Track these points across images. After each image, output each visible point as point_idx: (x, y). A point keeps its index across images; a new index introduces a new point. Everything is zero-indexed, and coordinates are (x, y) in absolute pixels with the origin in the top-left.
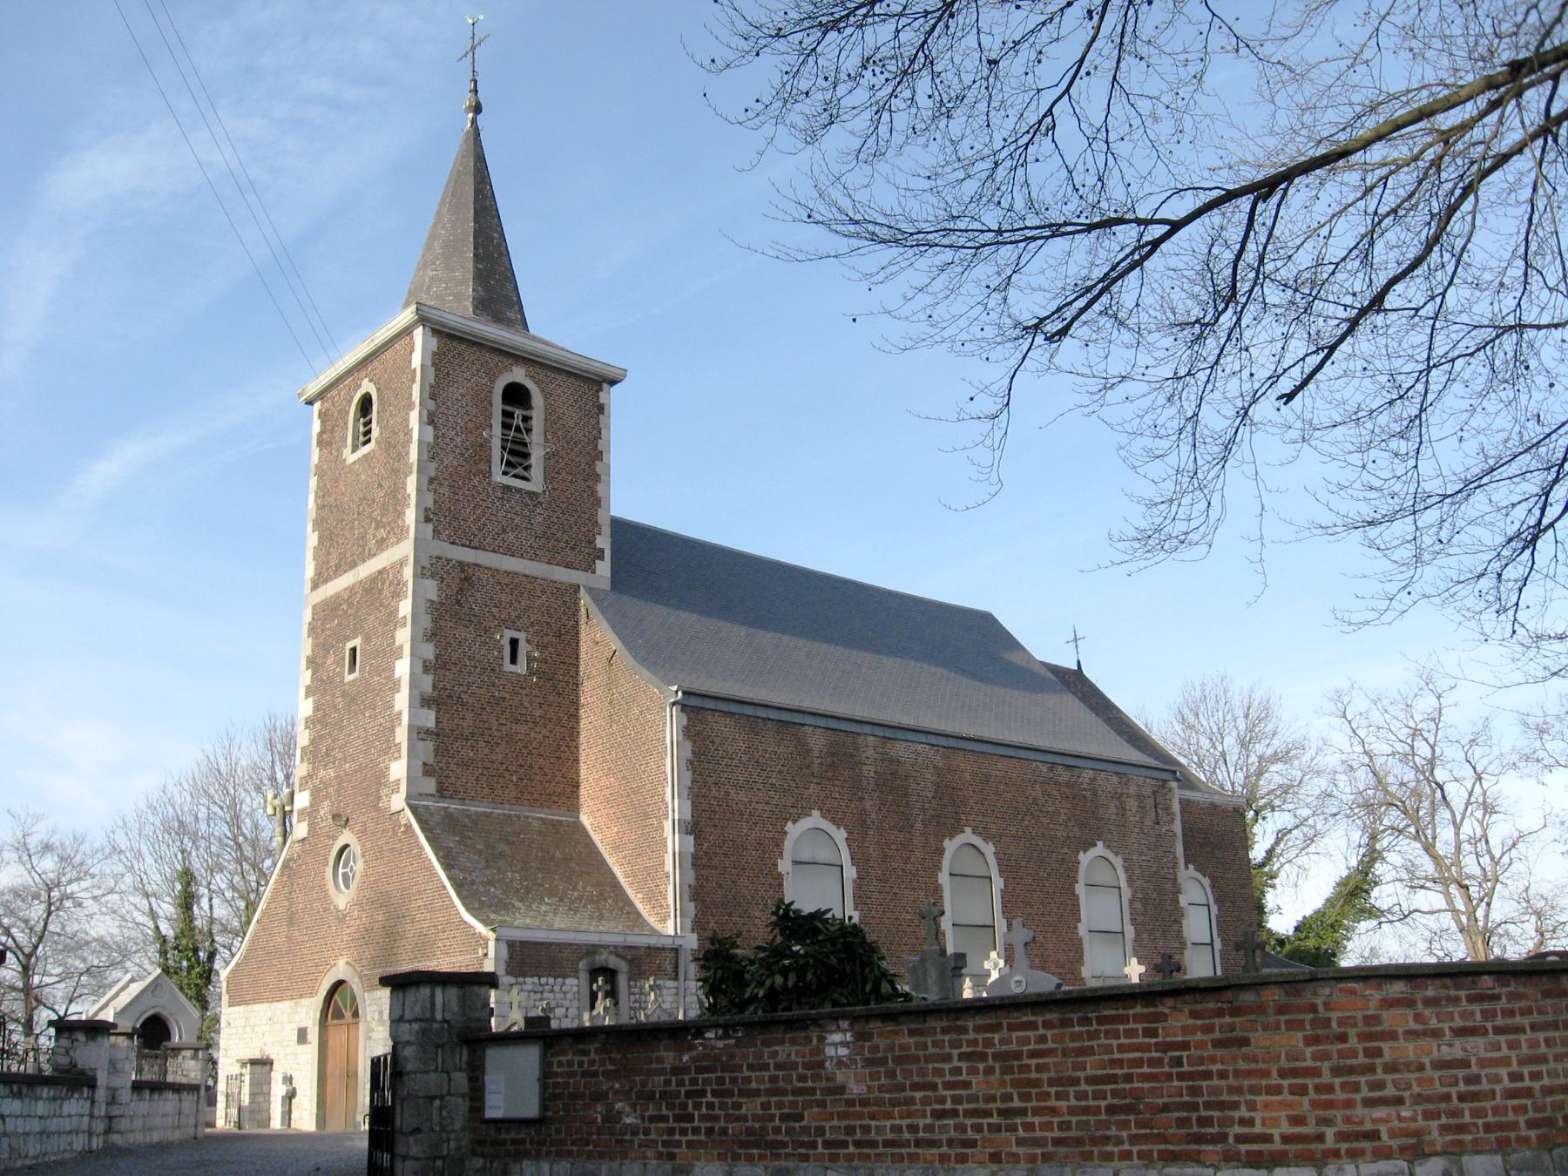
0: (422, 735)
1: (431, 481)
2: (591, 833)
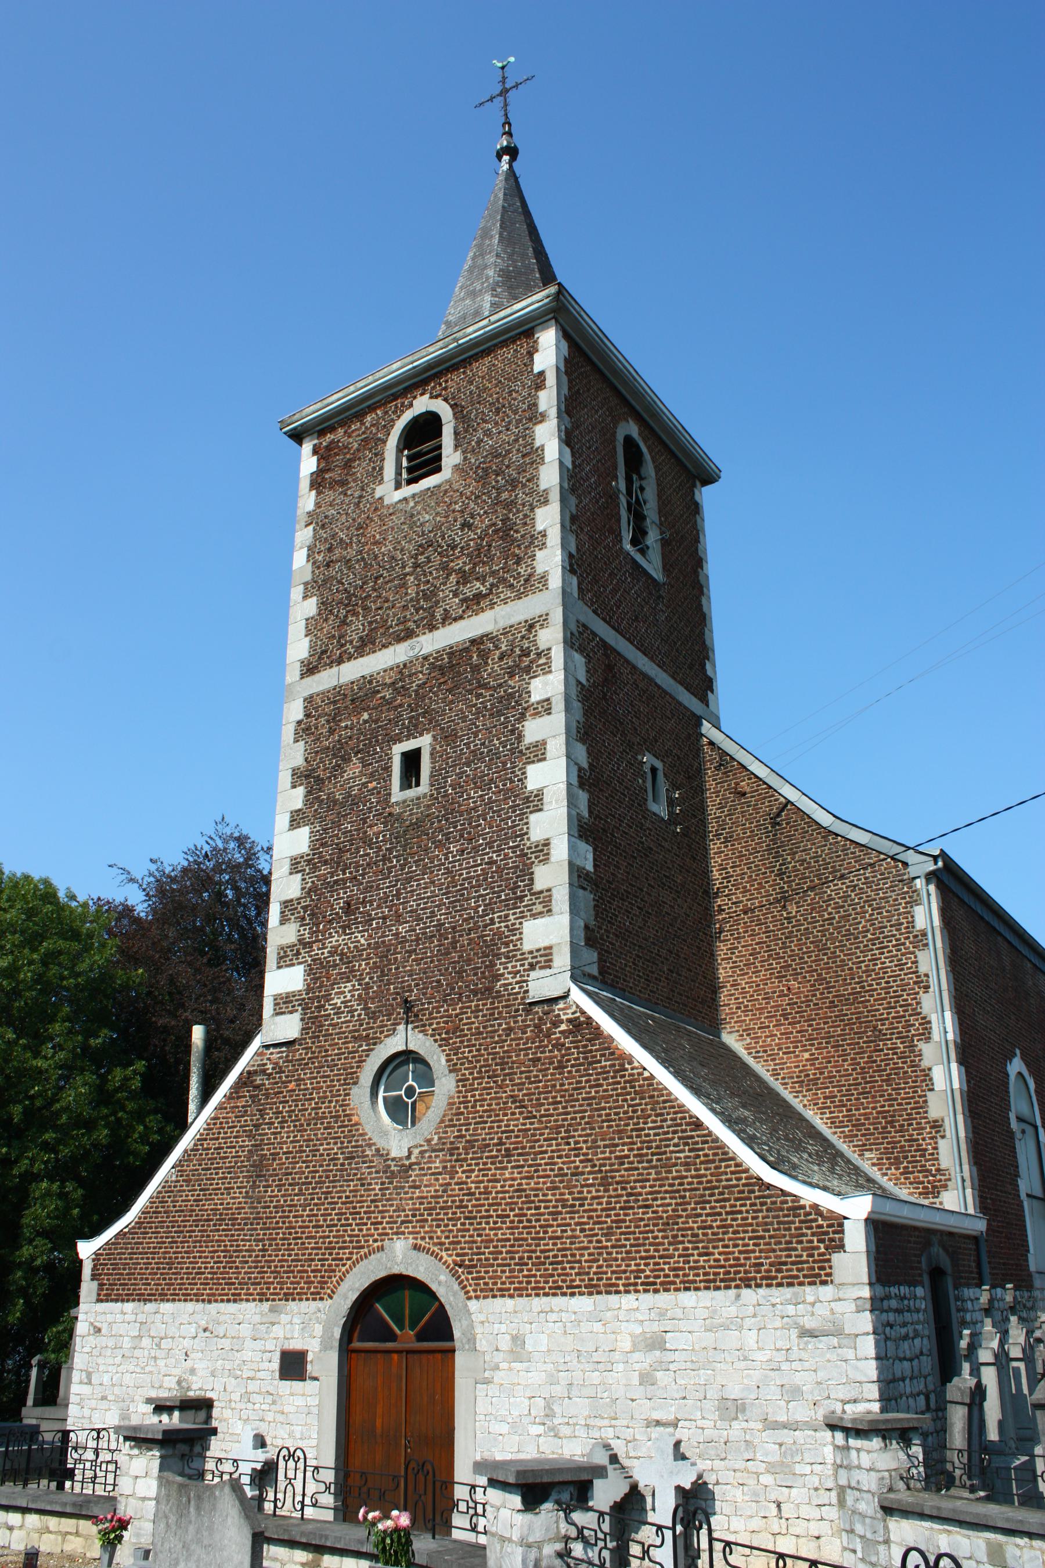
0: (585, 884)
1: (574, 519)
2: (750, 1061)
